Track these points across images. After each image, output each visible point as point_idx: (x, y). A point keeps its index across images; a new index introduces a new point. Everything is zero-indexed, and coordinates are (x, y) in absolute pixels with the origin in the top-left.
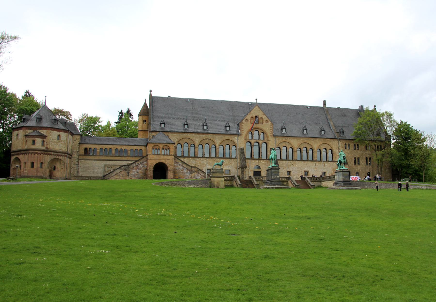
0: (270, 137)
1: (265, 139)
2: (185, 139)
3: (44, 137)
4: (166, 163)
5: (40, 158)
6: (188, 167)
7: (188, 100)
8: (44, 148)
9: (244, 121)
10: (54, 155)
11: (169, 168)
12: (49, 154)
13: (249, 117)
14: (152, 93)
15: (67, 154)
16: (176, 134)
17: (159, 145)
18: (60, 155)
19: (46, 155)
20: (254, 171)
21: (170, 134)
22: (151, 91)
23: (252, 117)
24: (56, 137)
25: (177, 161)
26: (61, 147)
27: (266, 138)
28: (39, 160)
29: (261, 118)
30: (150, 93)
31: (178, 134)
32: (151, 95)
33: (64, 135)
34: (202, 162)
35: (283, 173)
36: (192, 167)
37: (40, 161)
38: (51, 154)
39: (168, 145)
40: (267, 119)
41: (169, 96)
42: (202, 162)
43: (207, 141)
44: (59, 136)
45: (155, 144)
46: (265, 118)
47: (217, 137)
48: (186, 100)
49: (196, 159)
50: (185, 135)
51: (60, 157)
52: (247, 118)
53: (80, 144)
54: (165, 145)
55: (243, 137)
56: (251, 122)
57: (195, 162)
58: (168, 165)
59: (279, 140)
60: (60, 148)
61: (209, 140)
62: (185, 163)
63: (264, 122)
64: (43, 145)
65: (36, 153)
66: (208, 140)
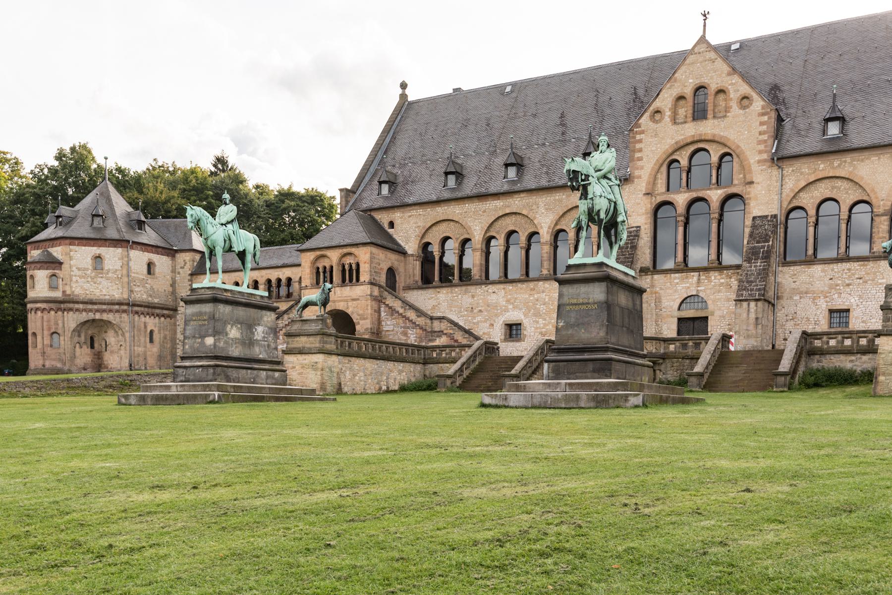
0: (756, 168)
1: (735, 182)
2: (443, 226)
3: (58, 264)
4: (349, 311)
5: (49, 321)
6: (421, 321)
7: (508, 89)
8: (58, 294)
9: (645, 120)
10: (85, 310)
11: (358, 327)
12: (71, 310)
13: (665, 101)
14: (407, 91)
15: (128, 304)
16: (414, 212)
17: (328, 253)
18: (97, 311)
19: (60, 313)
20: (679, 319)
21: (397, 216)
22: (404, 86)
23: (681, 98)
24: (88, 262)
25: (390, 301)
26: (108, 289)
27: (738, 178)
28: (45, 327)
29: (721, 91)
30: (400, 91)
31: (420, 211)
32: (403, 96)
33: (112, 256)
34: (493, 298)
35: (661, 317)
36: (432, 318)
37: (49, 329)
38: (77, 310)
39: (353, 250)
40: (745, 89)
41: (455, 90)
42: (493, 298)
43: (509, 224)
44: (98, 258)
45: (318, 253)
46: (737, 87)
47: (542, 200)
48: (499, 89)
49: (472, 289)
50: (441, 212)
51: (105, 317)
52: (657, 104)
53: (191, 275)
54: (346, 250)
55: (640, 185)
56: (674, 121)
57: (470, 300)
58: (355, 318)
59: (797, 175)
60: (104, 292)
61: (519, 217)
62: (412, 307)
63: (734, 105)
64: (53, 287)
65: (37, 309)
66: (513, 218)
